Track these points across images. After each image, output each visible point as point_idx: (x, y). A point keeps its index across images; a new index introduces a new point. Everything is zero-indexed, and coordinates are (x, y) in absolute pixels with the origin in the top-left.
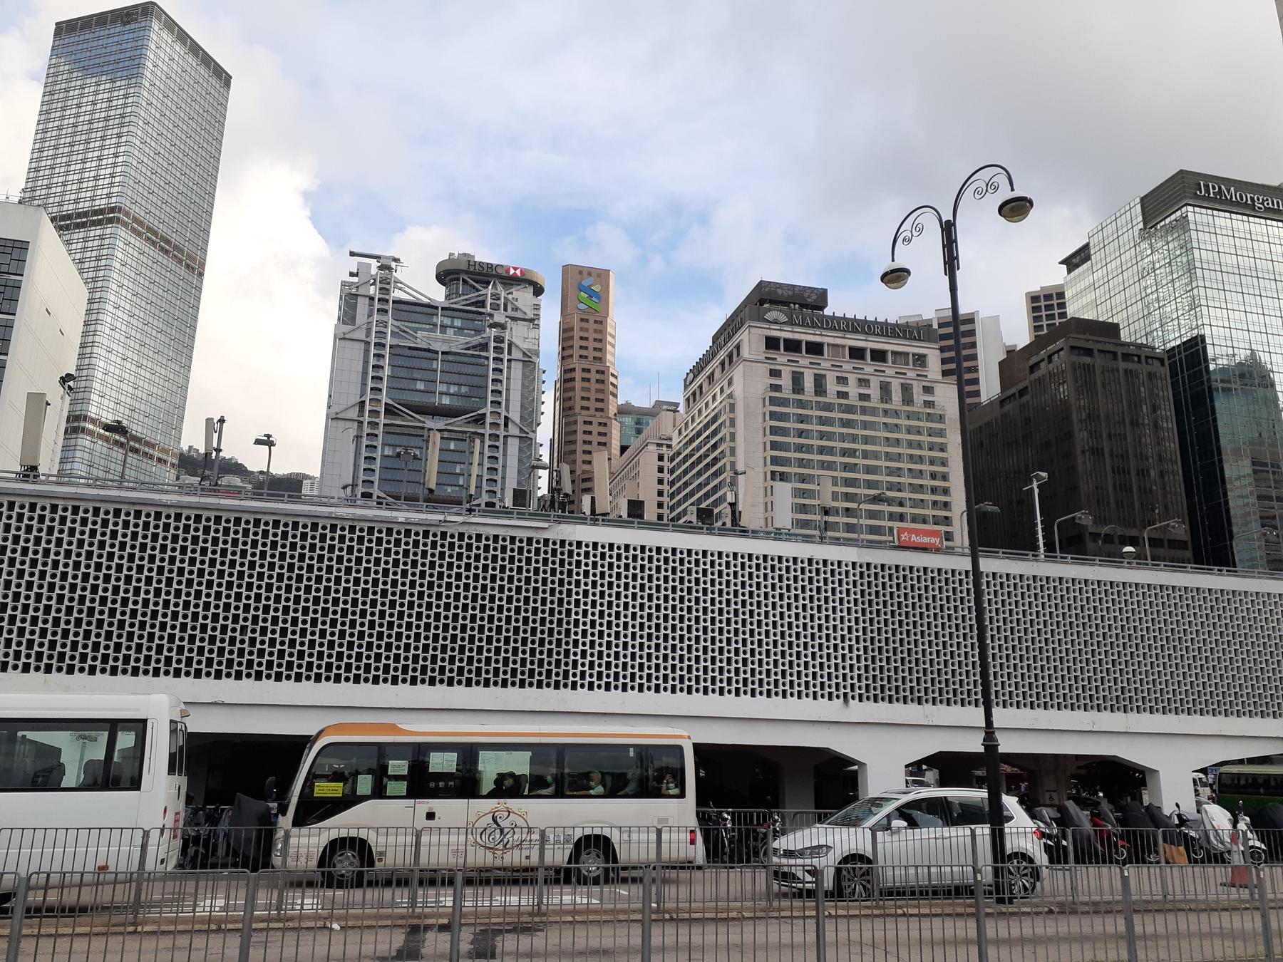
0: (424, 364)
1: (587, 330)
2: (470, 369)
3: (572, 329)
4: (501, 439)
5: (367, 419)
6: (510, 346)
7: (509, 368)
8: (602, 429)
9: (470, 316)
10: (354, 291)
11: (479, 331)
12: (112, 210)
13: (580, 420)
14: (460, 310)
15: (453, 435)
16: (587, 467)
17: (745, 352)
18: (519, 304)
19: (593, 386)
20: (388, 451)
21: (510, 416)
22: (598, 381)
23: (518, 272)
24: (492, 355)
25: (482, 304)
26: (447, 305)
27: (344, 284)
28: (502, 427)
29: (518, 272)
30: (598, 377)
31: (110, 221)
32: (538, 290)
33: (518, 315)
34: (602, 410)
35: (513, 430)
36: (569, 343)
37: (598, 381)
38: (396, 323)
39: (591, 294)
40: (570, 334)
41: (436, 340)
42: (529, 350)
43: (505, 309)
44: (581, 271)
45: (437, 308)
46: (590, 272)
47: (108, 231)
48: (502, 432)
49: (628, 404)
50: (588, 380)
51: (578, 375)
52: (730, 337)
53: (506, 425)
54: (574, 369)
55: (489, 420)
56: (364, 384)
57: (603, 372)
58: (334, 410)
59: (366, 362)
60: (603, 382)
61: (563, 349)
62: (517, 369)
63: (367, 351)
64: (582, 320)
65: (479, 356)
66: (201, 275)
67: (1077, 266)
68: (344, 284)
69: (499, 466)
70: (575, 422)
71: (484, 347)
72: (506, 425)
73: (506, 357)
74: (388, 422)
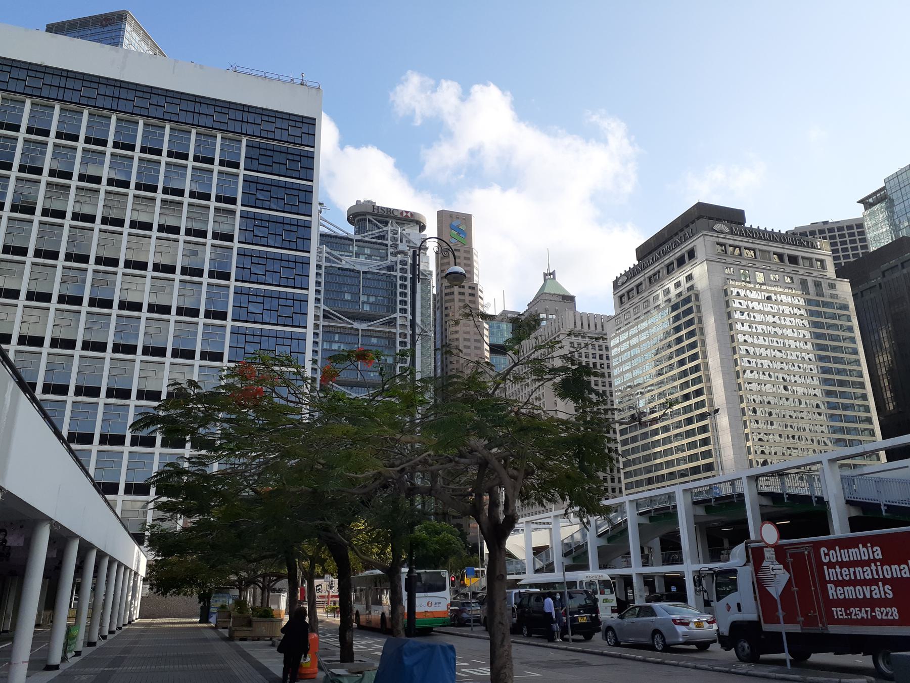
0: (350, 281)
9: (375, 246)
11: (384, 258)
14: (369, 242)
17: (700, 254)
18: (411, 238)
20: (326, 346)
22: (470, 295)
23: (409, 215)
25: (383, 237)
26: (359, 237)
30: (470, 291)
32: (422, 228)
33: (411, 245)
39: (460, 232)
43: (401, 241)
44: (451, 215)
45: (352, 240)
50: (463, 294)
52: (677, 245)
55: (399, 322)
57: (473, 288)
67: (872, 205)
71: (390, 268)
74: (326, 323)
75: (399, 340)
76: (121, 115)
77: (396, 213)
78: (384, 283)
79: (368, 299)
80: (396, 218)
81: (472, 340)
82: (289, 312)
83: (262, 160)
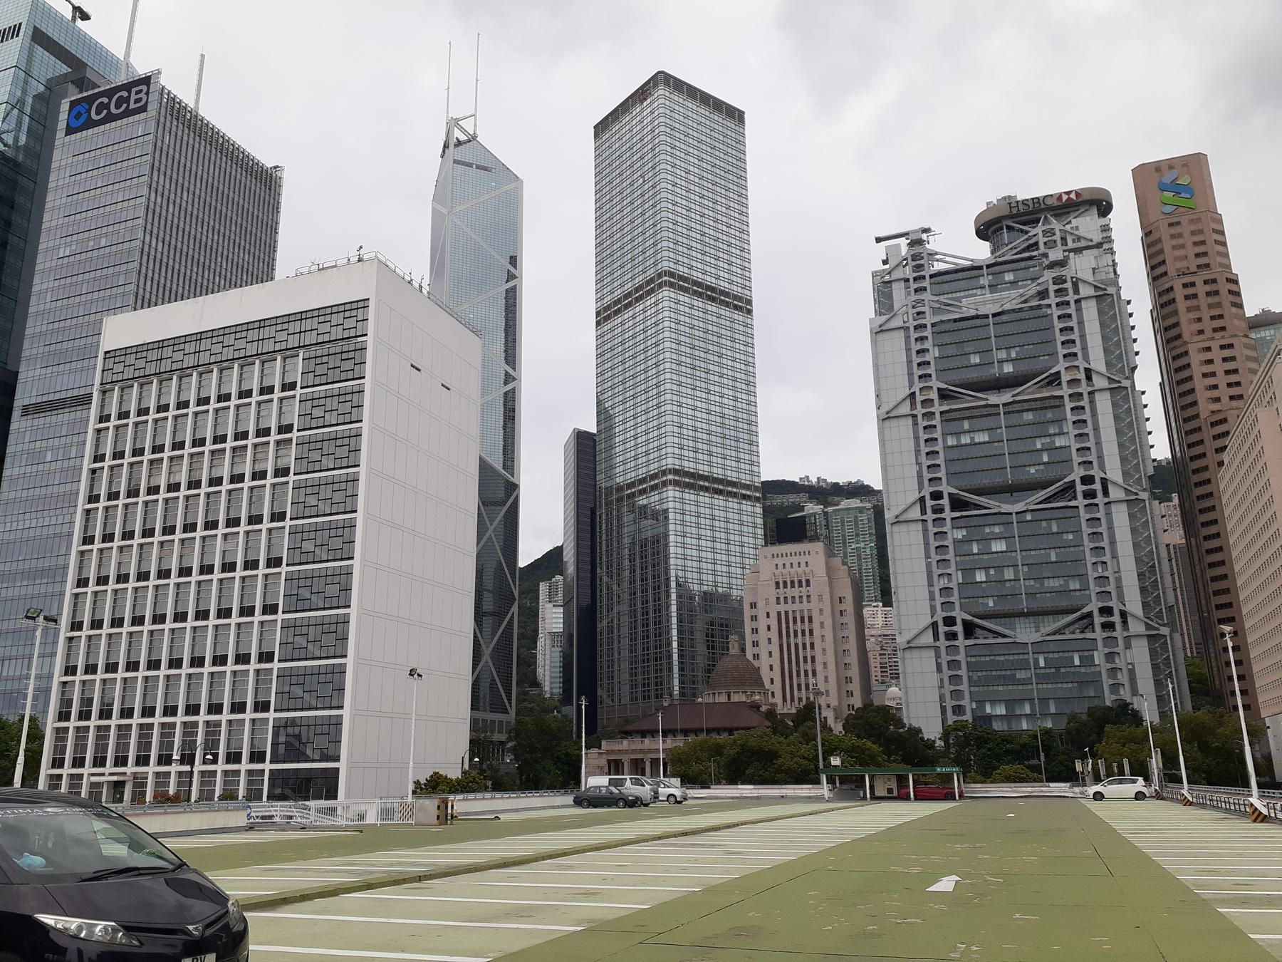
1: (1180, 235)
2: (1032, 325)
3: (1159, 241)
4: (1086, 396)
5: (920, 411)
6: (1075, 285)
7: (1079, 310)
8: (1227, 353)
9: (1023, 264)
10: (887, 278)
12: (660, 276)
13: (1192, 349)
15: (1026, 406)
16: (1216, 407)
18: (1081, 232)
19: (1203, 301)
20: (951, 441)
21: (1093, 366)
22: (1208, 294)
23: (1073, 196)
24: (1053, 300)
27: (874, 274)
28: (1084, 382)
29: (1073, 196)
30: (1208, 288)
31: (660, 286)
33: (1083, 244)
34: (1223, 329)
35: (1099, 382)
36: (1159, 259)
37: (1208, 294)
38: (936, 298)
39: (1177, 189)
40: (1158, 247)
41: (984, 303)
42: (1102, 282)
44: (1158, 167)
45: (980, 268)
46: (1171, 164)
47: (660, 296)
48: (1084, 388)
49: (1265, 313)
50: (1195, 296)
51: (1179, 293)
53: (1089, 378)
54: (1172, 288)
55: (1065, 378)
56: (910, 374)
57: (1214, 281)
58: (885, 408)
59: (908, 350)
60: (1217, 293)
61: (1153, 268)
62: (1090, 311)
63: (907, 338)
64: (1171, 225)
65: (1039, 307)
66: (749, 312)
68: (874, 274)
69: (1089, 430)
70: (1186, 353)
71: (1043, 294)
72: (1089, 378)
73: (1071, 297)
75: (1069, 405)
76: (200, 369)
77: (1049, 202)
78: (1026, 323)
79: (1008, 354)
80: (1051, 209)
81: (1220, 373)
82: (337, 543)
83: (319, 370)
